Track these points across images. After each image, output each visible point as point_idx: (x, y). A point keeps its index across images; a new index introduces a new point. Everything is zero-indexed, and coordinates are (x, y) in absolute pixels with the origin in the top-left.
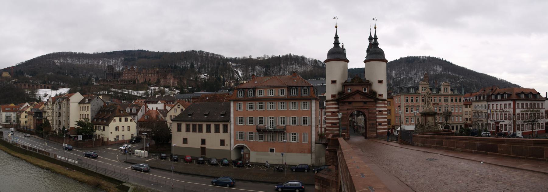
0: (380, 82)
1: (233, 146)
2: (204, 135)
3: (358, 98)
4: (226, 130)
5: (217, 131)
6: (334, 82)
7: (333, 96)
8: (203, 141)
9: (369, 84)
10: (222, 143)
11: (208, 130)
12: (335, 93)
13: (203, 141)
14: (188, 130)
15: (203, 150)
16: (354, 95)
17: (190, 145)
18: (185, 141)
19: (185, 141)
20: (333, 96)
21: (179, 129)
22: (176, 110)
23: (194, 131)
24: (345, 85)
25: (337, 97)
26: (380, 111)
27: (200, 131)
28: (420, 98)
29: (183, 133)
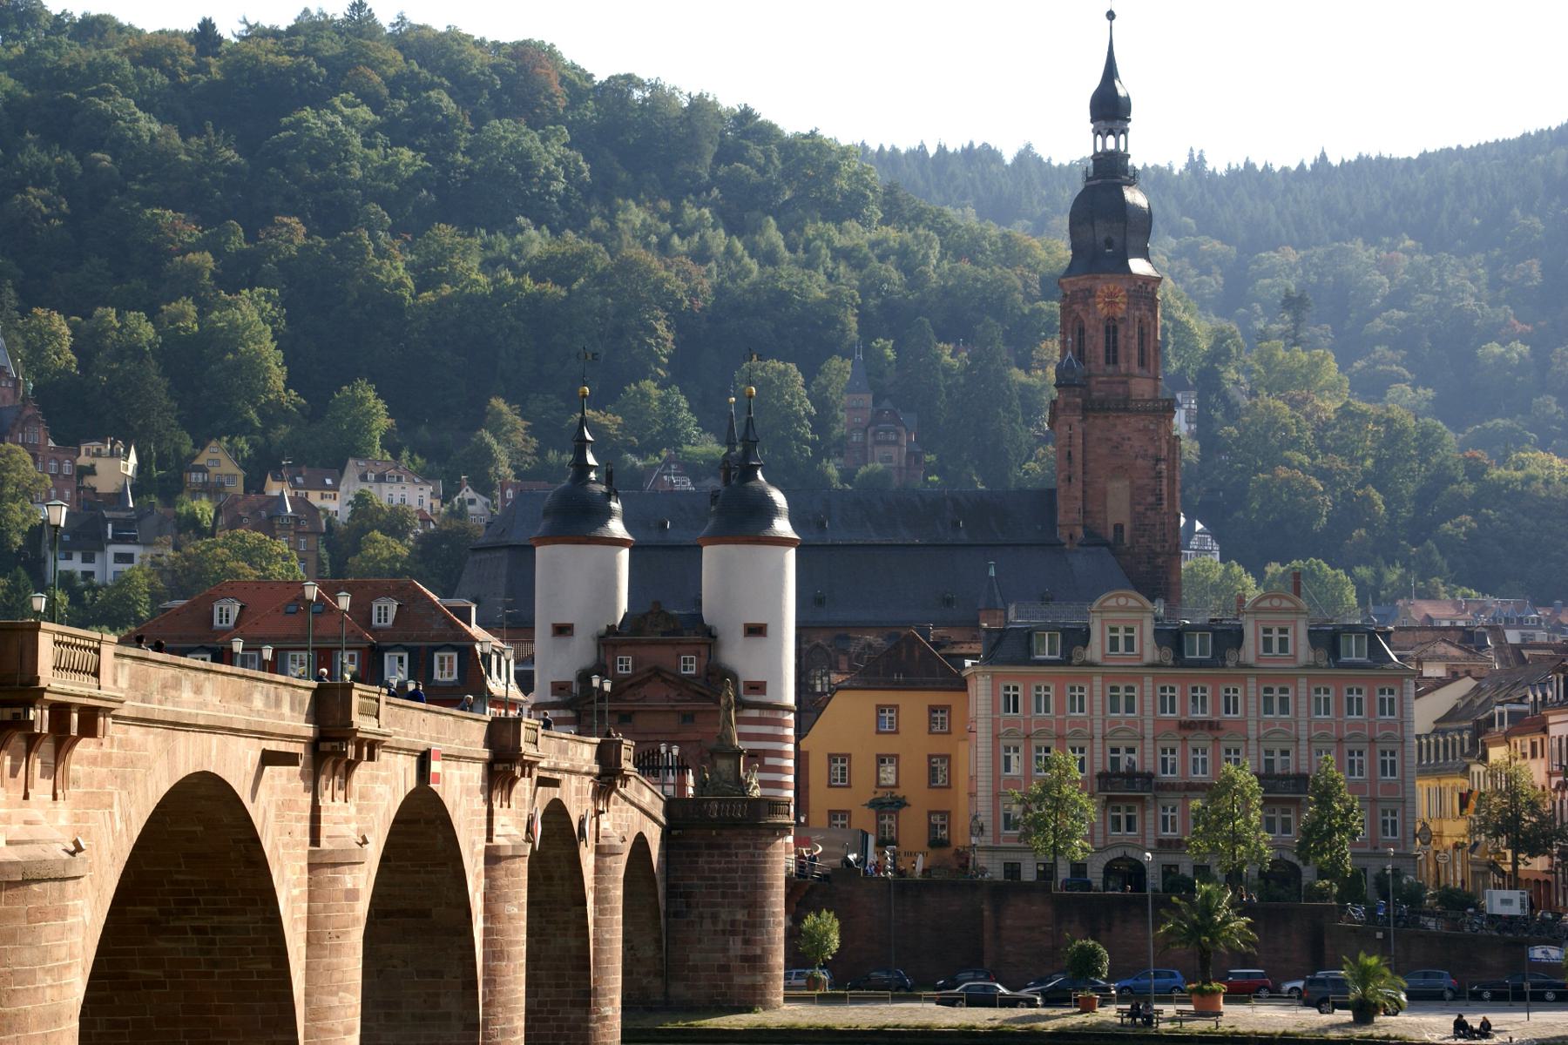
0: (756, 631)
6: (562, 630)
7: (558, 688)
9: (709, 638)
12: (569, 675)
16: (641, 684)
20: (558, 688)
24: (610, 640)
25: (576, 689)
26: (754, 755)
28: (1097, 690)
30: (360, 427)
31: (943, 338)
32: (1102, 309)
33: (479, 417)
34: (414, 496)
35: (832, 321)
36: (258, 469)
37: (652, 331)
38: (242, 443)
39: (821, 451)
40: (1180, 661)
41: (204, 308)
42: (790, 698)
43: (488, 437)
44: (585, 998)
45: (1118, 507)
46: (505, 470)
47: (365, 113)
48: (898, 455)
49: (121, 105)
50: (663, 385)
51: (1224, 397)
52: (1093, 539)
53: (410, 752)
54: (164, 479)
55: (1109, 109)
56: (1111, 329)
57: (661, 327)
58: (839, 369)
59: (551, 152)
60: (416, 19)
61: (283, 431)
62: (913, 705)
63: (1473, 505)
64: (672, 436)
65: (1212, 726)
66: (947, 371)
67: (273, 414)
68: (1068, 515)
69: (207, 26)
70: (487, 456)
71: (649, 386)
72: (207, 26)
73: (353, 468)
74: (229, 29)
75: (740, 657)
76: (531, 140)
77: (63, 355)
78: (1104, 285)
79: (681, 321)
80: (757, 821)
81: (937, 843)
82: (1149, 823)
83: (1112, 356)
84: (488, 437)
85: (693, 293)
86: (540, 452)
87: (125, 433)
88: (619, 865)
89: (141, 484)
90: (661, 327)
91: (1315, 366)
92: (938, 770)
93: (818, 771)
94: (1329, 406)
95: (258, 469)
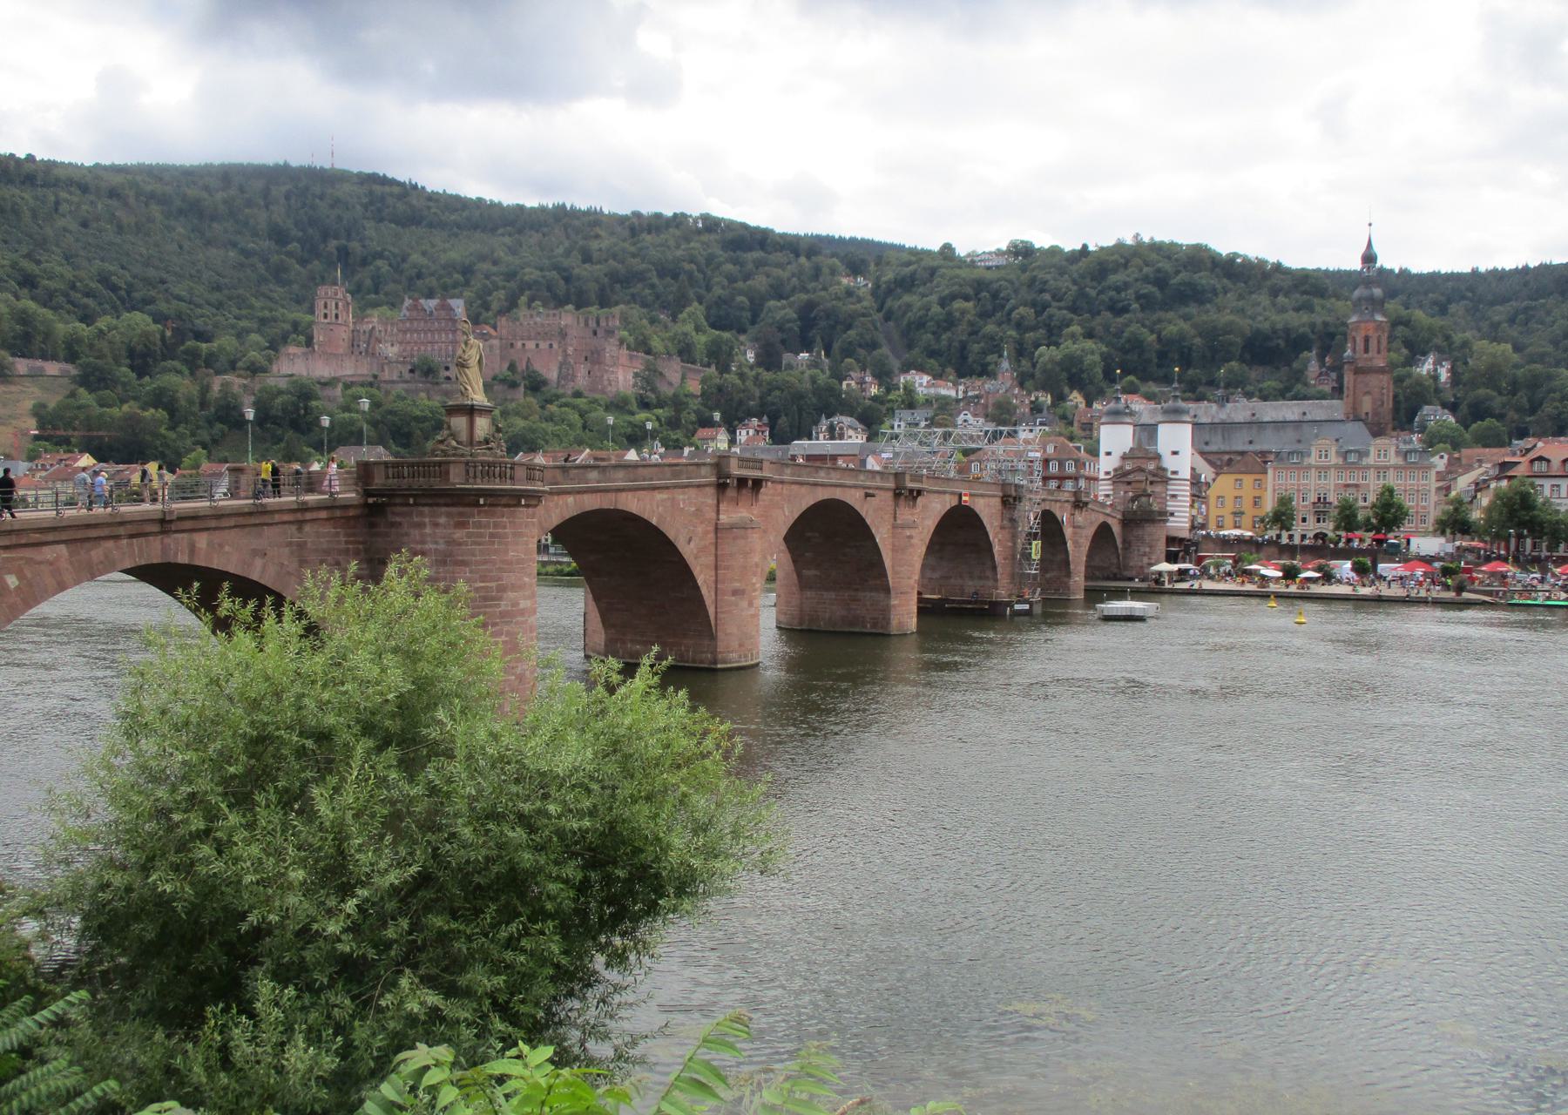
0: (1175, 453)
3: (1141, 477)
6: (1108, 454)
9: (1158, 457)
12: (1110, 469)
24: (1124, 457)
26: (1174, 496)
32: (1363, 333)
53: (952, 493)
55: (1369, 258)
56: (1367, 340)
60: (1157, 239)
62: (1248, 480)
65: (1356, 486)
69: (1085, 247)
72: (1085, 247)
74: (1092, 248)
83: (1366, 350)
88: (1090, 531)
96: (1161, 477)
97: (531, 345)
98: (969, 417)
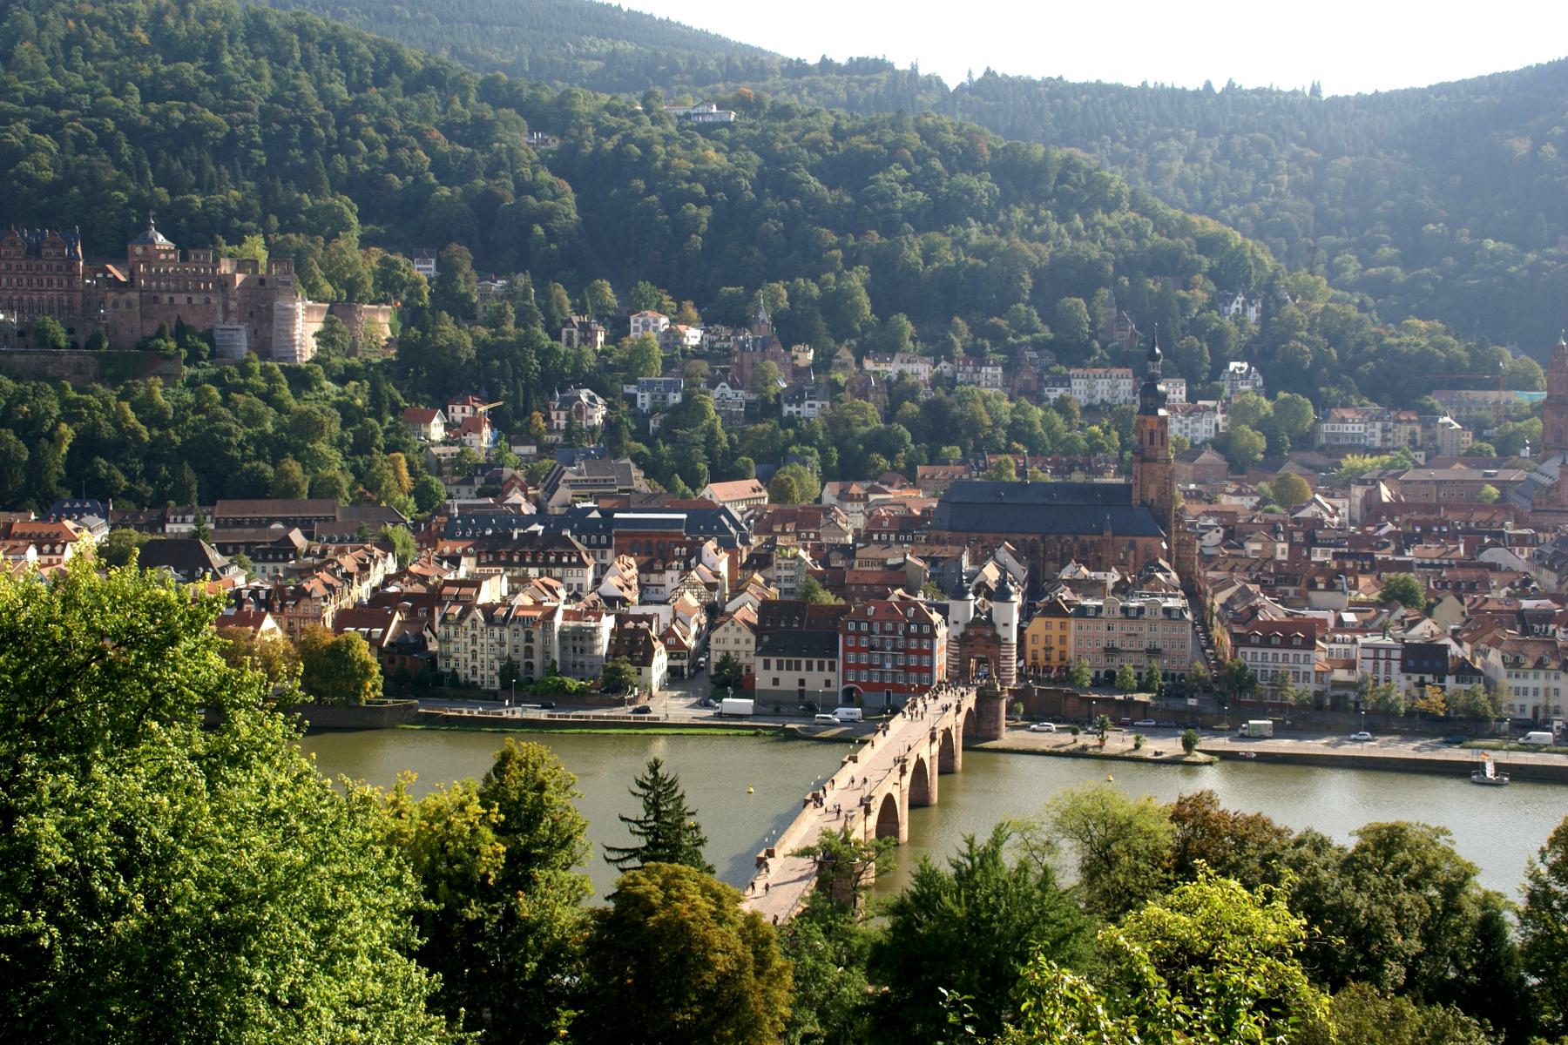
1: (841, 688)
2: (803, 674)
3: (980, 640)
4: (832, 668)
5: (821, 668)
8: (802, 682)
9: (994, 626)
10: (828, 683)
11: (809, 668)
13: (802, 682)
14: (780, 667)
15: (801, 692)
17: (783, 686)
18: (776, 681)
19: (776, 681)
21: (767, 666)
22: (727, 630)
23: (789, 668)
24: (968, 626)
27: (798, 668)
28: (1104, 625)
29: (774, 672)
30: (900, 332)
31: (1150, 275)
33: (948, 321)
34: (922, 370)
35: (1101, 268)
36: (860, 354)
37: (1022, 280)
38: (854, 342)
39: (1093, 336)
40: (1127, 617)
41: (839, 275)
42: (1014, 640)
43: (953, 336)
44: (953, 757)
45: (1152, 493)
46: (960, 349)
47: (904, 173)
48: (1127, 335)
49: (803, 174)
50: (1028, 304)
51: (1275, 297)
52: (1143, 503)
54: (823, 363)
56: (1152, 434)
57: (1026, 277)
58: (1105, 293)
59: (982, 186)
61: (869, 336)
62: (1056, 622)
63: (1373, 357)
64: (1030, 330)
66: (1151, 292)
67: (866, 327)
68: (1135, 496)
70: (952, 343)
71: (1021, 306)
73: (898, 356)
75: (1001, 631)
76: (974, 183)
77: (784, 303)
78: (1149, 419)
79: (1035, 274)
80: (998, 697)
81: (1062, 659)
82: (1117, 661)
84: (953, 336)
85: (1041, 260)
86: (975, 340)
87: (809, 340)
89: (817, 366)
90: (1026, 277)
91: (1317, 283)
92: (1063, 640)
93: (1029, 640)
94: (1318, 306)
95: (860, 354)
96: (997, 641)
97: (181, 299)
98: (729, 392)
